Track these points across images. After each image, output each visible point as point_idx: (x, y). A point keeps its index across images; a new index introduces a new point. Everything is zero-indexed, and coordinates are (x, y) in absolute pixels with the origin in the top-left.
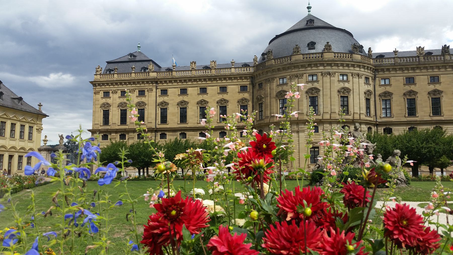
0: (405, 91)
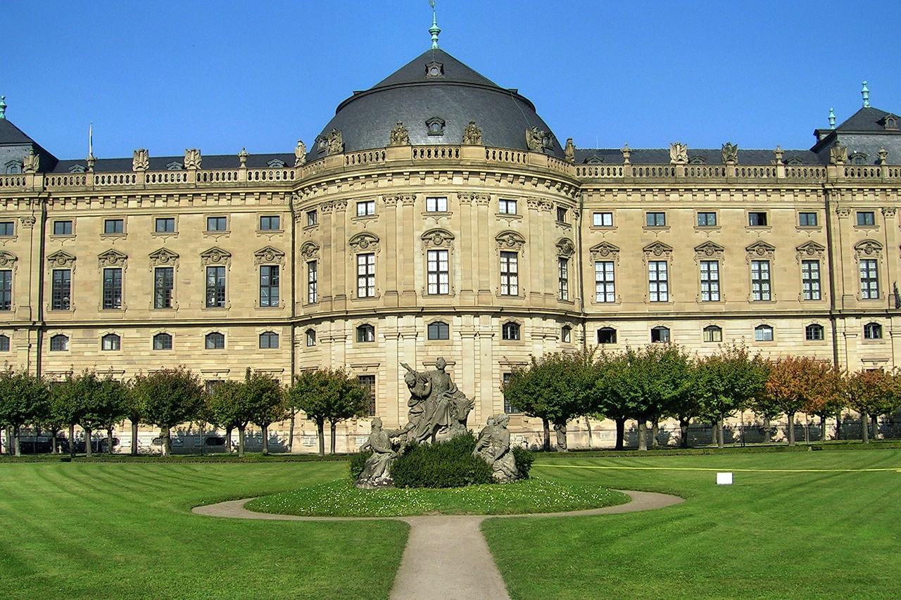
0: (645, 244)
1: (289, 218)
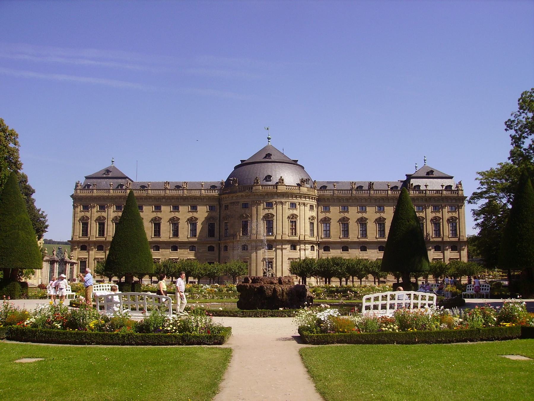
1: (218, 207)
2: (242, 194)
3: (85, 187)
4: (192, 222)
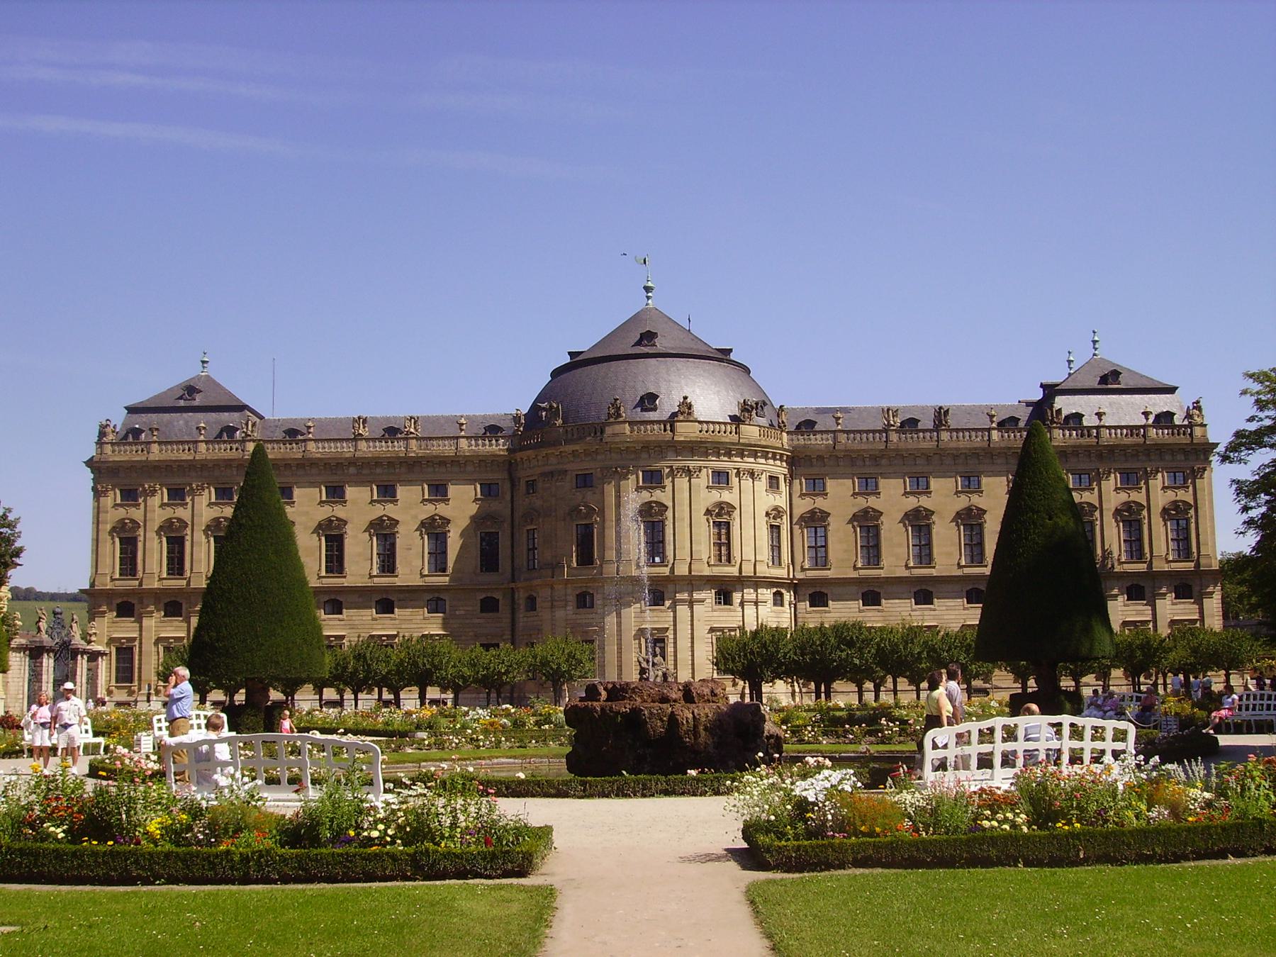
1: (507, 485)
2: (577, 447)
3: (126, 437)
4: (435, 530)
